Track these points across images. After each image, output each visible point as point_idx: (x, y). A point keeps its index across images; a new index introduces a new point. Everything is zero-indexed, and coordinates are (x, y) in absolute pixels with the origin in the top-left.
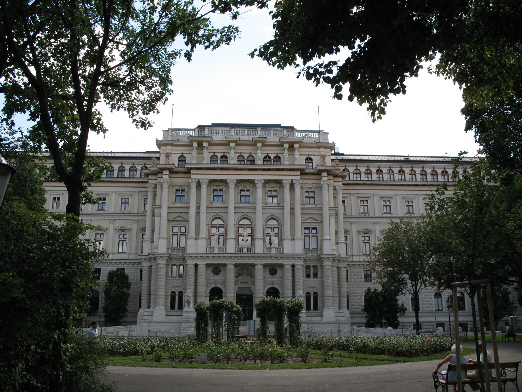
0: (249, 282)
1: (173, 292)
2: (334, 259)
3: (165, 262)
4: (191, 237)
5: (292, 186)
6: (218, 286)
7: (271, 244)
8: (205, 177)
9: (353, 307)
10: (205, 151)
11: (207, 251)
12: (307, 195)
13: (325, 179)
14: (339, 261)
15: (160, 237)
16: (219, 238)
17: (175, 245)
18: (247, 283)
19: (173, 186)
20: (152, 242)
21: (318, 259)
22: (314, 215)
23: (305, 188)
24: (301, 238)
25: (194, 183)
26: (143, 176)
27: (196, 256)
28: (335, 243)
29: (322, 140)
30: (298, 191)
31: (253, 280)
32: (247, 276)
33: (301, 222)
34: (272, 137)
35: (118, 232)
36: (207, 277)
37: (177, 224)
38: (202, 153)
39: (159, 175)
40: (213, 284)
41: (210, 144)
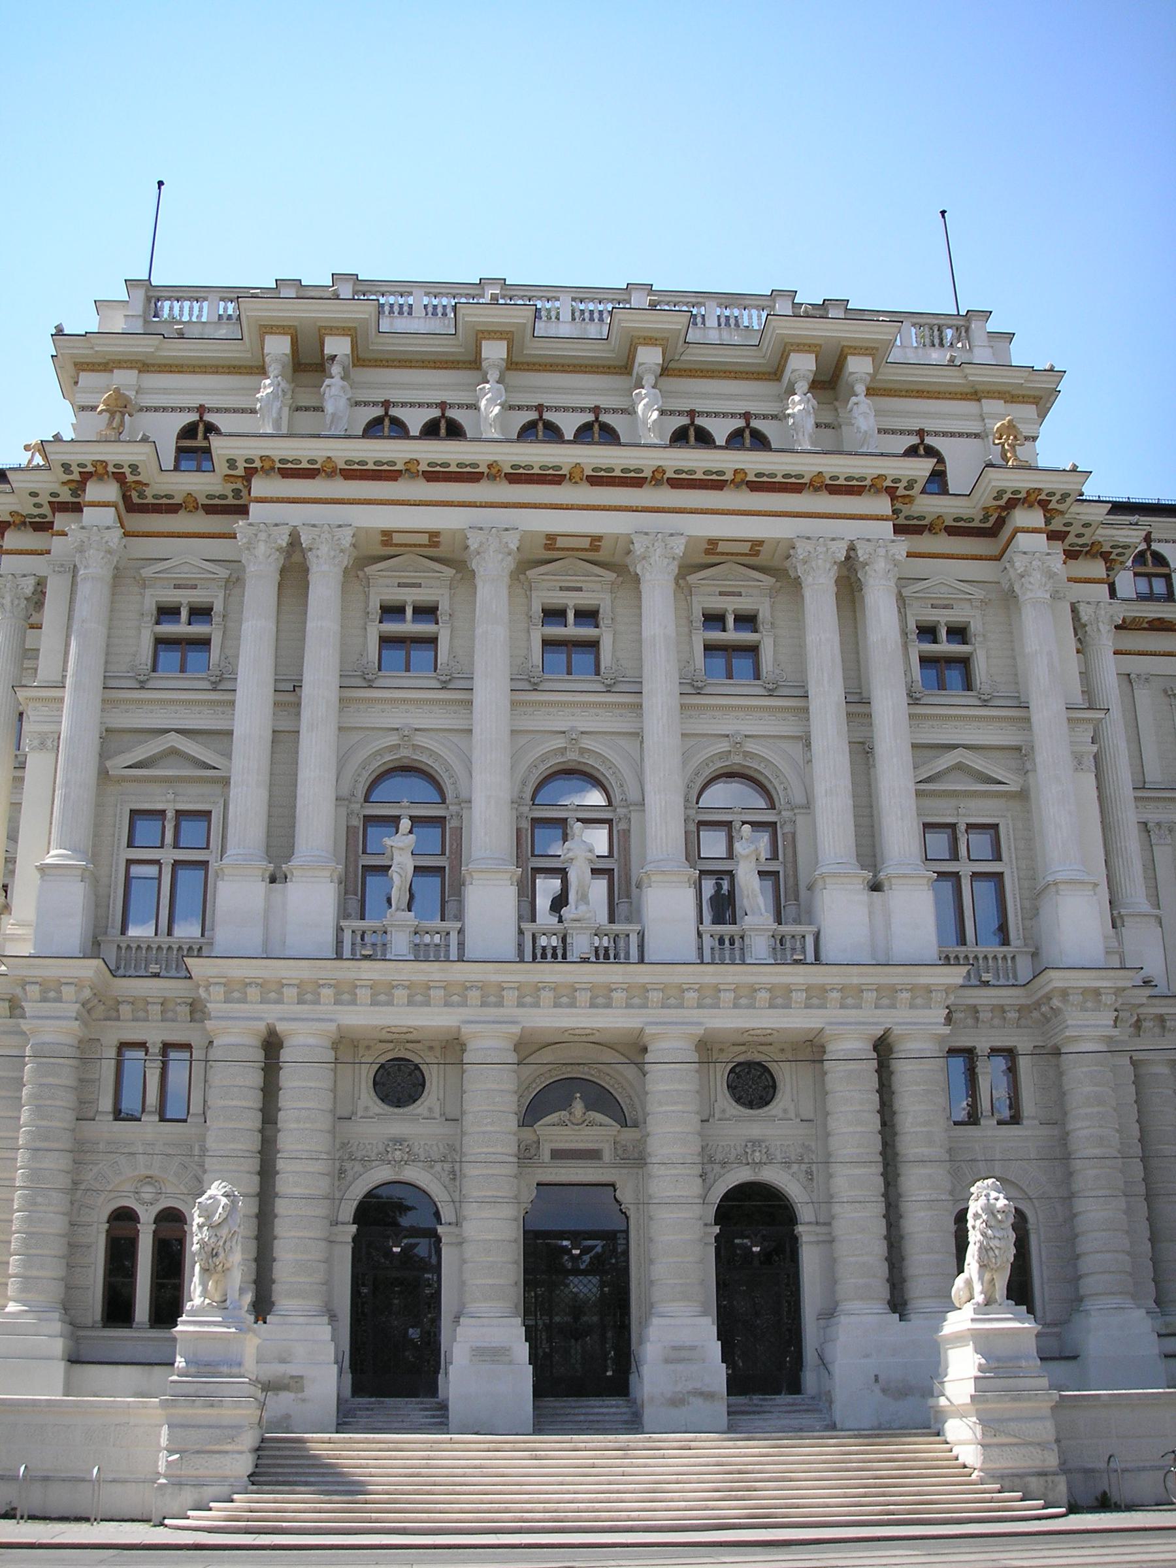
0: (607, 1156)
1: (124, 1217)
6: (411, 1174)
18: (593, 1155)
21: (1021, 1009)
25: (261, 549)
31: (629, 1135)
39: (61, 521)
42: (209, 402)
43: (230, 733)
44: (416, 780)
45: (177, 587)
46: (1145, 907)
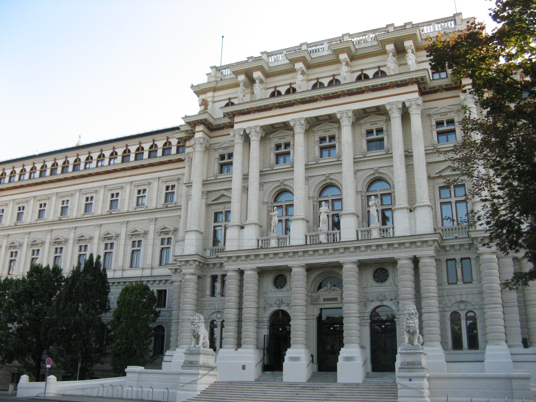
6: (283, 308)
10: (257, 87)
15: (188, 229)
18: (336, 299)
23: (435, 117)
24: (429, 203)
25: (237, 136)
30: (416, 120)
35: (160, 235)
37: (220, 208)
40: (274, 306)
41: (267, 75)
42: (231, 96)
44: (285, 195)
45: (224, 150)
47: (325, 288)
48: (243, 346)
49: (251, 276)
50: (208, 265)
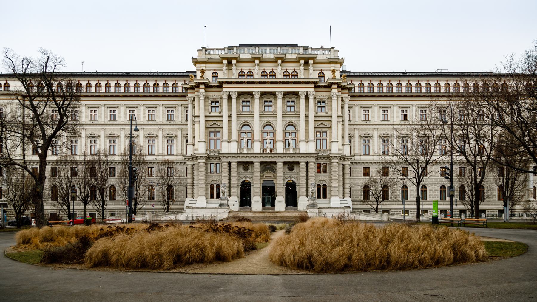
2: (340, 158)
3: (204, 161)
4: (225, 140)
5: (307, 97)
6: (247, 179)
7: (289, 146)
8: (235, 90)
9: (354, 196)
11: (238, 152)
12: (319, 105)
13: (335, 90)
14: (345, 159)
15: (200, 140)
16: (248, 142)
17: (212, 148)
18: (271, 177)
19: (208, 98)
20: (194, 145)
22: (325, 122)
23: (318, 99)
24: (314, 140)
25: (225, 95)
26: (184, 92)
27: (229, 156)
28: (341, 145)
29: (332, 57)
30: (311, 101)
31: (275, 174)
32: (270, 172)
33: (314, 128)
34: (291, 55)
36: (238, 173)
37: (213, 130)
38: (232, 70)
39: (196, 89)
41: (238, 62)
43: (222, 121)
46: (348, 143)
47: (267, 172)
48: (231, 196)
49: (234, 165)
50: (209, 158)
